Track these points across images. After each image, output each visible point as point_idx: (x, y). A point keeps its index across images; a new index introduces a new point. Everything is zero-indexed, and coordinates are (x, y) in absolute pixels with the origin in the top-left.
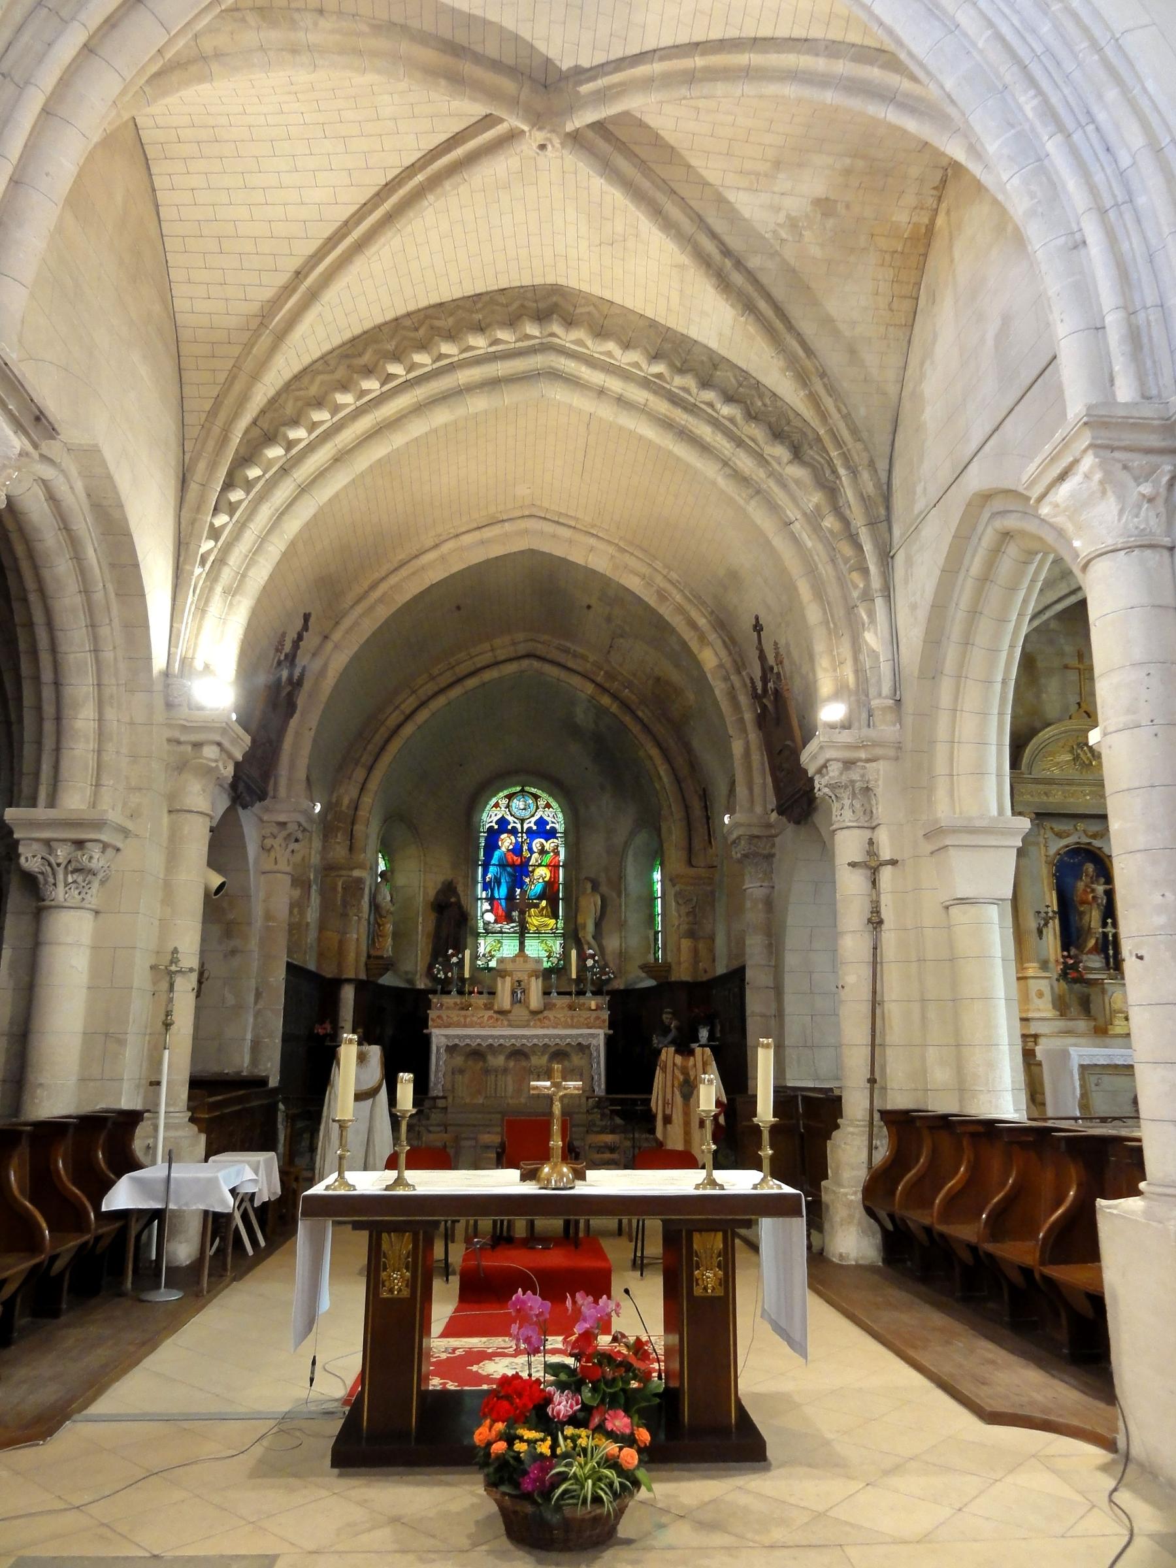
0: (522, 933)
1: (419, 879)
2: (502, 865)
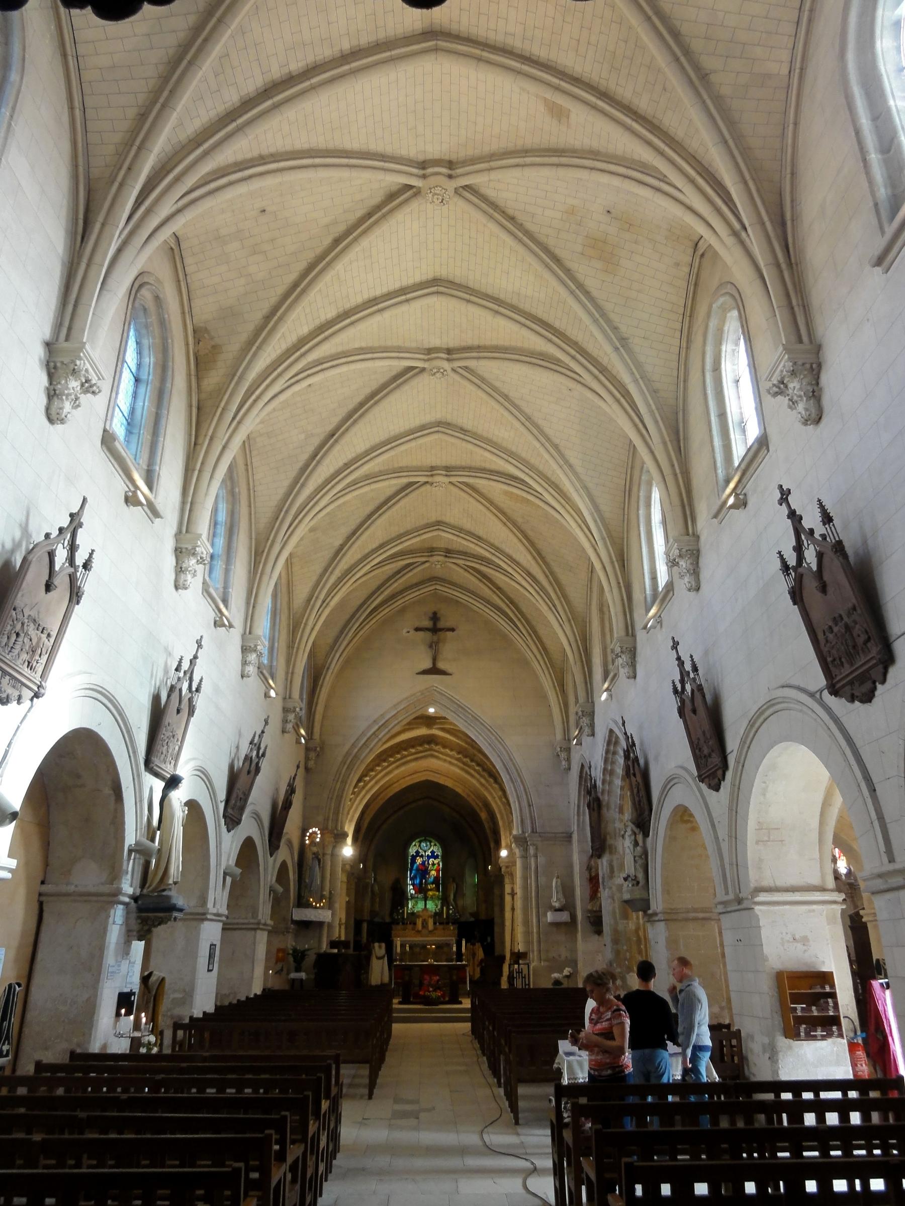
0: (425, 899)
1: (387, 878)
2: (418, 869)
